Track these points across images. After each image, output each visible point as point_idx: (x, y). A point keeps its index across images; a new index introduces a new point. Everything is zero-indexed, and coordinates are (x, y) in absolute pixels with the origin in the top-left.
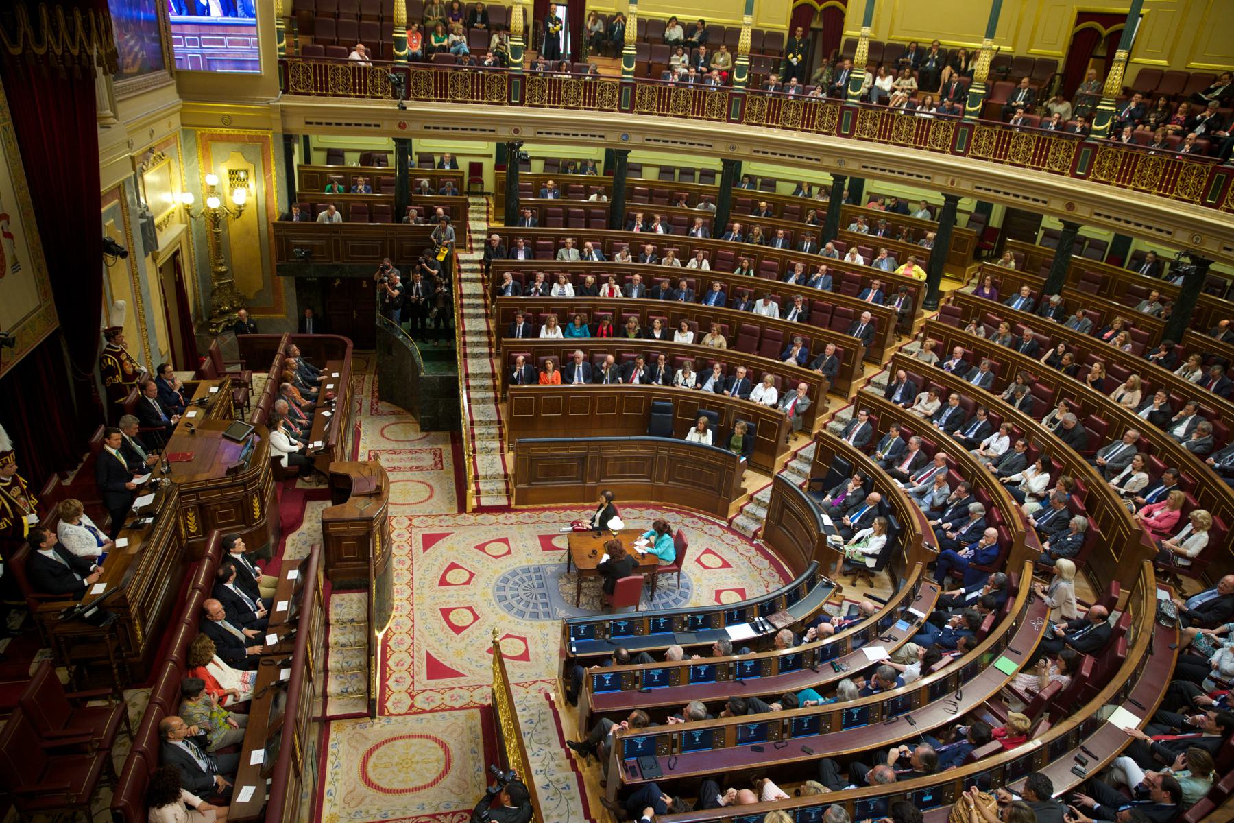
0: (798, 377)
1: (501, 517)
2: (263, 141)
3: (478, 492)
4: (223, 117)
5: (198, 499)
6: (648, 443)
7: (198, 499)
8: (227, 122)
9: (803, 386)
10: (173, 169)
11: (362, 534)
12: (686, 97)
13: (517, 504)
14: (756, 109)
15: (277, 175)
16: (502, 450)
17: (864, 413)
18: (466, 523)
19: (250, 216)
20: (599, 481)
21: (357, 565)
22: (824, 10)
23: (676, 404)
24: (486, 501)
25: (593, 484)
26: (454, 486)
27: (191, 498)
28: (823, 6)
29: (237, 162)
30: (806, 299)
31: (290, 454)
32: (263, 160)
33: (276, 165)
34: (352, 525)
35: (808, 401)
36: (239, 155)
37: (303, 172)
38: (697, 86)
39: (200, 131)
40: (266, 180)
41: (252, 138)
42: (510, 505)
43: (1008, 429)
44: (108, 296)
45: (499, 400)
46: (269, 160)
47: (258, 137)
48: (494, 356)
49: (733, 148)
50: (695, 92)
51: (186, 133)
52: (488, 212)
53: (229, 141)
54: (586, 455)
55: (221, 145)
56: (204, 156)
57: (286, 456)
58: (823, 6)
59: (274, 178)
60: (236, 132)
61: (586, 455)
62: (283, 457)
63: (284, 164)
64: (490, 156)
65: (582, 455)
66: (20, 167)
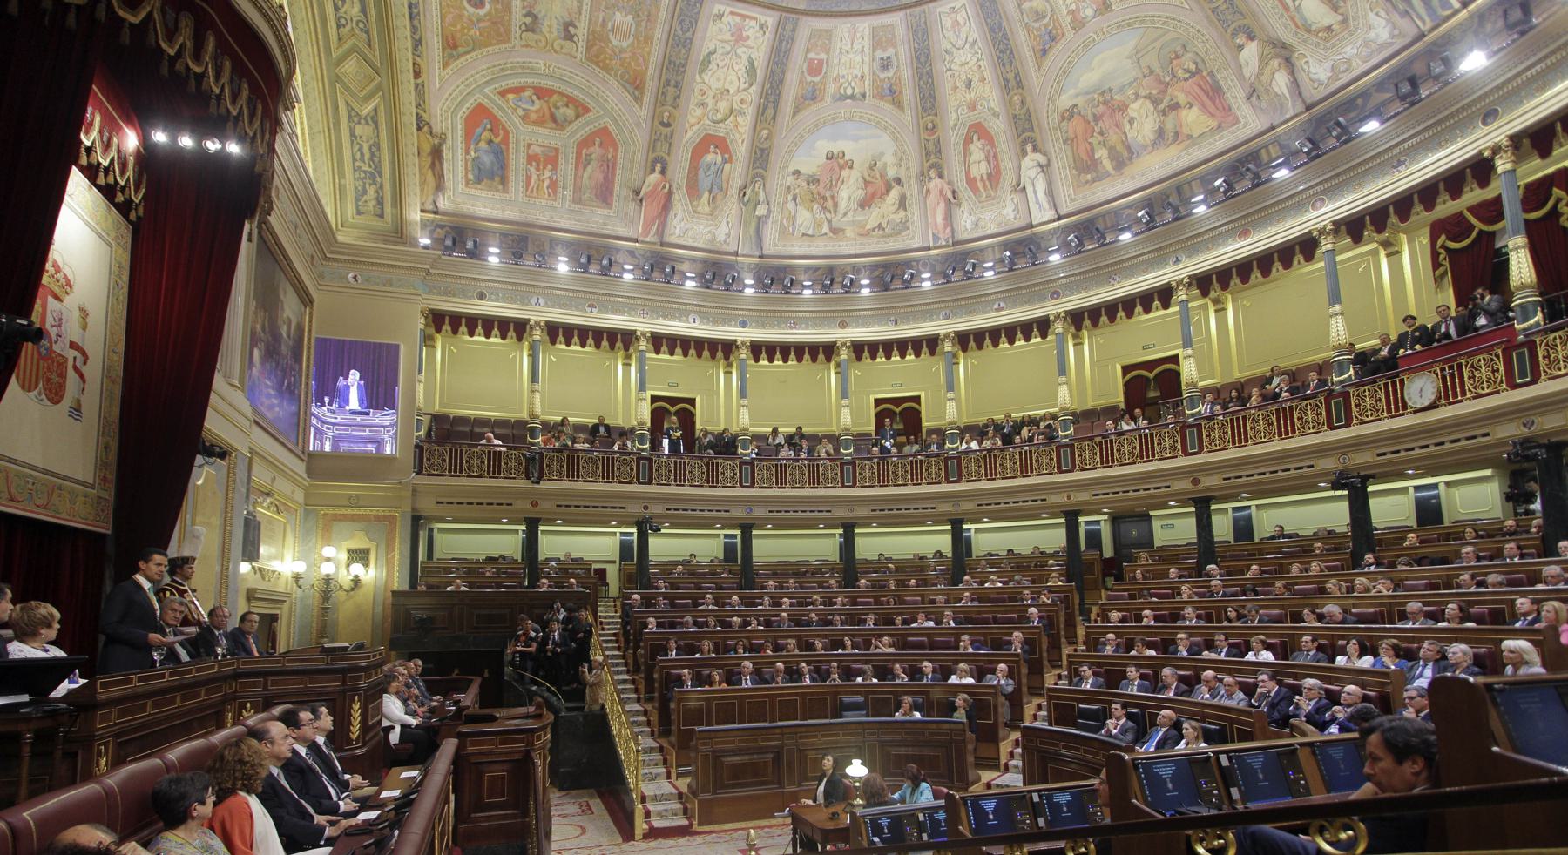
0: (991, 662)
1: (682, 841)
2: (390, 520)
3: (648, 814)
4: (350, 497)
5: (265, 688)
6: (853, 726)
7: (265, 688)
8: (353, 501)
9: (1002, 666)
10: (287, 539)
11: (517, 757)
12: (801, 469)
13: (699, 824)
14: (867, 473)
15: (401, 553)
16: (669, 777)
17: (1085, 668)
18: (638, 849)
19: (364, 596)
20: (800, 785)
21: (505, 817)
22: (901, 412)
23: (866, 700)
24: (658, 823)
25: (794, 789)
26: (611, 823)
27: (254, 685)
28: (900, 408)
29: (359, 542)
30: (937, 665)
31: (404, 727)
32: (387, 546)
33: (400, 544)
34: (504, 742)
35: (1011, 681)
36: (362, 533)
37: (426, 568)
38: (810, 460)
39: (323, 511)
40: (387, 559)
41: (378, 518)
42: (691, 825)
43: (1263, 642)
44: (189, 510)
45: (656, 733)
46: (394, 539)
47: (385, 516)
48: (642, 701)
49: (852, 511)
50: (809, 465)
51: (307, 513)
52: (615, 606)
53: (353, 521)
54: (782, 747)
55: (342, 524)
56: (323, 537)
57: (398, 729)
58: (900, 408)
59: (397, 557)
60: (362, 511)
61: (782, 747)
62: (393, 727)
63: (409, 542)
64: (614, 562)
65: (776, 746)
66: (122, 309)
